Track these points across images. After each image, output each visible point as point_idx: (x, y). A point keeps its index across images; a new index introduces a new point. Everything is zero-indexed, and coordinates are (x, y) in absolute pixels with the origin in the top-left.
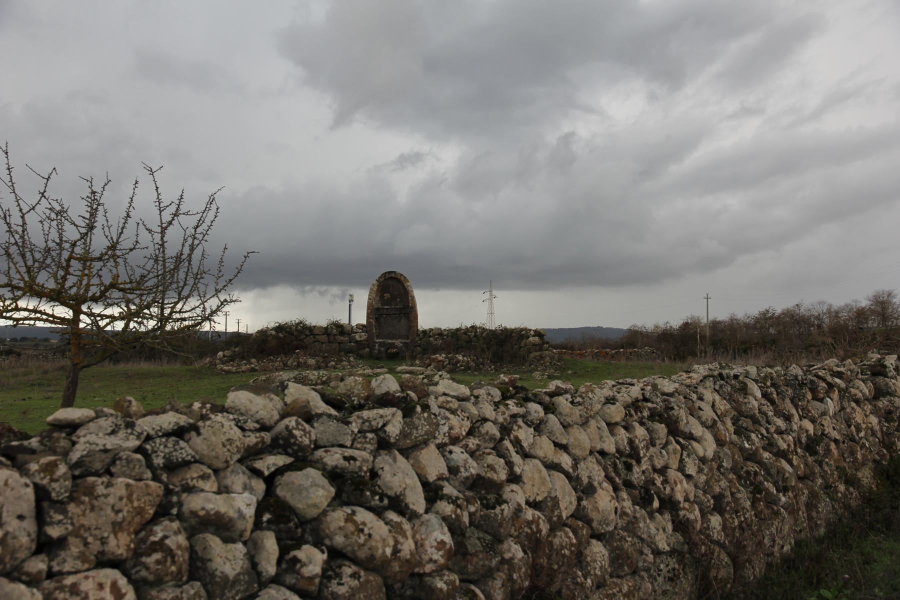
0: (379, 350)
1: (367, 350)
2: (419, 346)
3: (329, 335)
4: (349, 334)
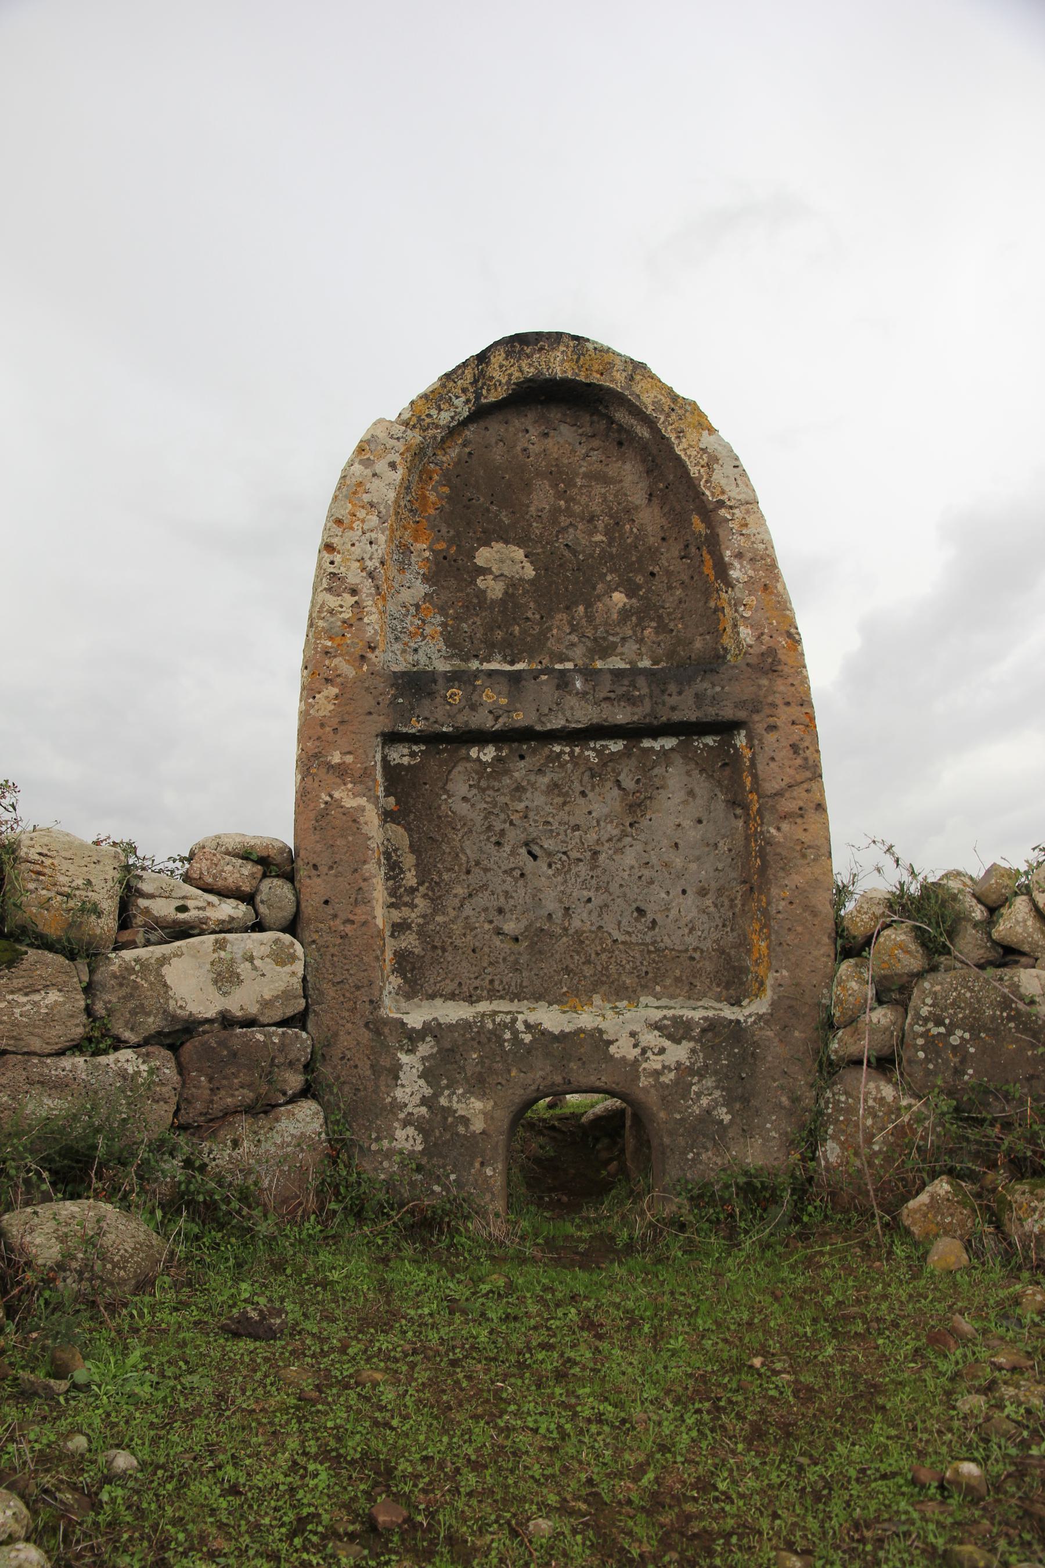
0: (439, 1128)
1: (305, 1120)
2: (884, 1064)
4: (78, 949)
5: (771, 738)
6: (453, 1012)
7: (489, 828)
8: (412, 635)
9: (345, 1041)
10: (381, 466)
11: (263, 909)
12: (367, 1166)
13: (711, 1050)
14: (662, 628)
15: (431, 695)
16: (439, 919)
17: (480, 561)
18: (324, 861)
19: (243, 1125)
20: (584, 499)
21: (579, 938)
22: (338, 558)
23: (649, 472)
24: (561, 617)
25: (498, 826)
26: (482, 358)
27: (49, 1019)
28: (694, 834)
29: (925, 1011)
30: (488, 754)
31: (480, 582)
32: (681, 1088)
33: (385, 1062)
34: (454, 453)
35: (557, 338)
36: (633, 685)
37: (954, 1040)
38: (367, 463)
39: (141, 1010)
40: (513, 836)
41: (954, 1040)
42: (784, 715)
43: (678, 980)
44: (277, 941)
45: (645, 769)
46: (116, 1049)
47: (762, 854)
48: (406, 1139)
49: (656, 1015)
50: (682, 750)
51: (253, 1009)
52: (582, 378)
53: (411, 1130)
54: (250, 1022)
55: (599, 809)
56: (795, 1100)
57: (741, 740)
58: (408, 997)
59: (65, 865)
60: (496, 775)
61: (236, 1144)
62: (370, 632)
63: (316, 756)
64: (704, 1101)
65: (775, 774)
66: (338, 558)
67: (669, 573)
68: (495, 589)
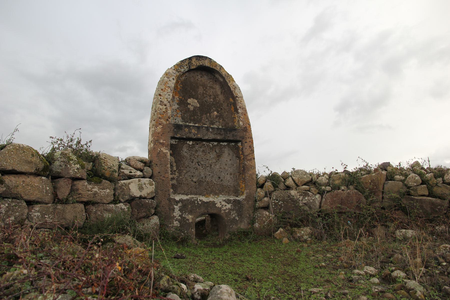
0: (183, 220)
1: (155, 220)
2: (266, 208)
3: (55, 177)
4: (111, 180)
5: (246, 144)
6: (185, 197)
7: (191, 159)
8: (175, 116)
9: (163, 203)
10: (171, 79)
11: (145, 173)
12: (168, 230)
13: (235, 206)
14: (223, 120)
15: (181, 129)
16: (181, 177)
17: (188, 102)
19: (145, 221)
20: (209, 92)
21: (208, 183)
22: (162, 97)
23: (221, 88)
24: (204, 116)
25: (192, 158)
26: (190, 59)
27: (108, 196)
28: (230, 162)
29: (274, 198)
30: (191, 143)
31: (189, 106)
32: (229, 213)
33: (172, 207)
34: (183, 78)
35: (206, 58)
36: (221, 131)
37: (280, 203)
38: (168, 78)
39: (124, 194)
40: (195, 161)
41: (280, 203)
42: (248, 140)
43: (226, 192)
44: (150, 181)
45: (221, 149)
46: (119, 203)
47: (243, 167)
48: (176, 223)
49: (224, 198)
50: (228, 145)
51: (146, 195)
52: (211, 67)
53: (177, 222)
54: (145, 198)
55: (212, 156)
56: (250, 215)
57: (240, 144)
58: (174, 194)
59: (109, 161)
60: (192, 148)
61: (143, 224)
62: (169, 114)
63: (157, 140)
64: (234, 216)
65: (247, 152)
66: (162, 97)
67: (225, 109)
68: (192, 108)
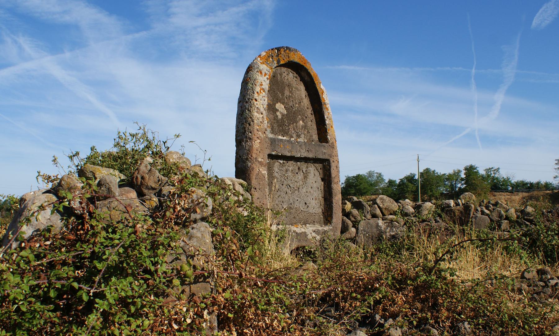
18: (257, 188)
30: (281, 162)
49: (314, 229)
55: (300, 178)
